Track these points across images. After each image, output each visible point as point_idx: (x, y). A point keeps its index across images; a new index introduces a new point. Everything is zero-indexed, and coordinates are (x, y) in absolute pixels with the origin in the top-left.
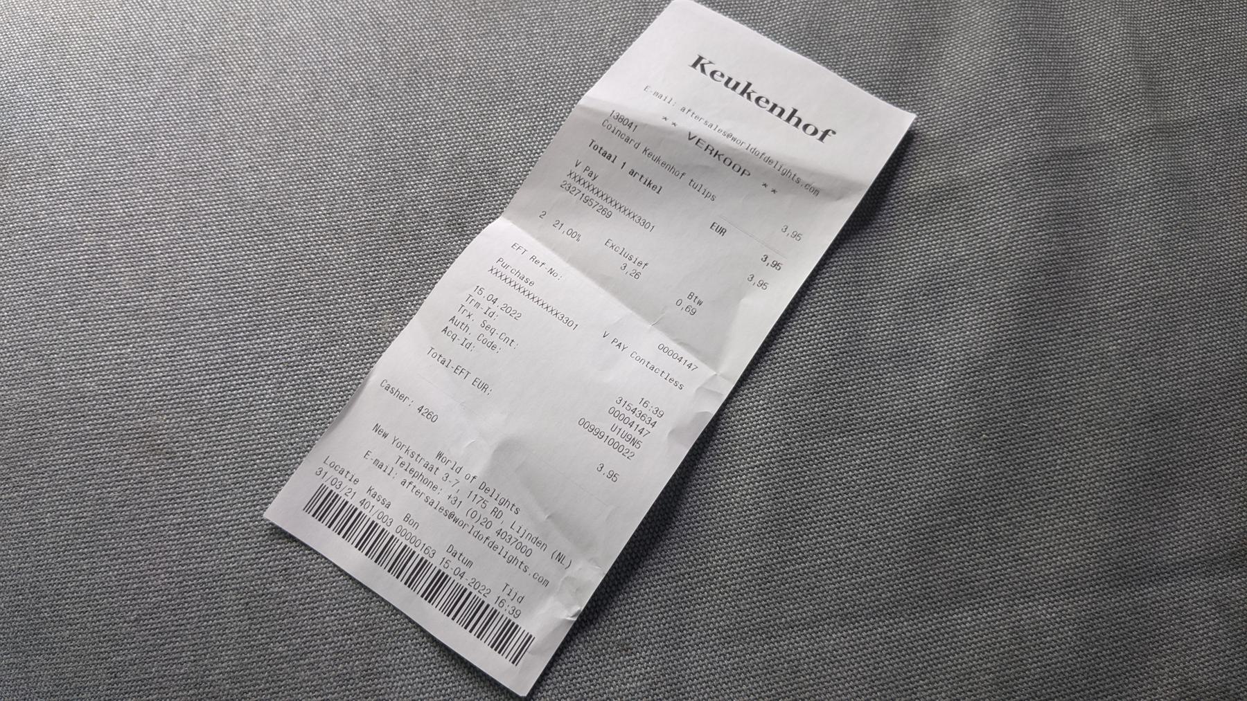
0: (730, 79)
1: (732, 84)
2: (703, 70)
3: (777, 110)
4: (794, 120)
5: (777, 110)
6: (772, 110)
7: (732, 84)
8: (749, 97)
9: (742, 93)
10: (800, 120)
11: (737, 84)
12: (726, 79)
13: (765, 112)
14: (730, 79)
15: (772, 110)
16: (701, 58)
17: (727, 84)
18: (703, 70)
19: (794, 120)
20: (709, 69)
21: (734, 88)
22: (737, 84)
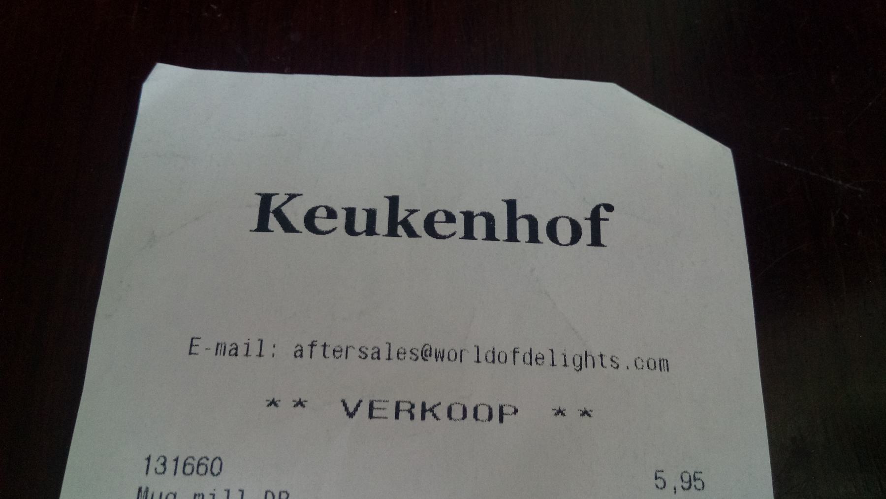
0: (351, 213)
1: (360, 223)
2: (288, 227)
3: (480, 224)
4: (523, 227)
5: (480, 224)
6: (469, 234)
7: (360, 223)
8: (411, 233)
9: (392, 232)
10: (533, 222)
11: (371, 215)
12: (341, 220)
13: (458, 243)
14: (351, 213)
15: (469, 234)
16: (266, 199)
17: (350, 229)
18: (288, 227)
19: (523, 227)
20: (295, 213)
21: (371, 230)
22: (371, 215)
